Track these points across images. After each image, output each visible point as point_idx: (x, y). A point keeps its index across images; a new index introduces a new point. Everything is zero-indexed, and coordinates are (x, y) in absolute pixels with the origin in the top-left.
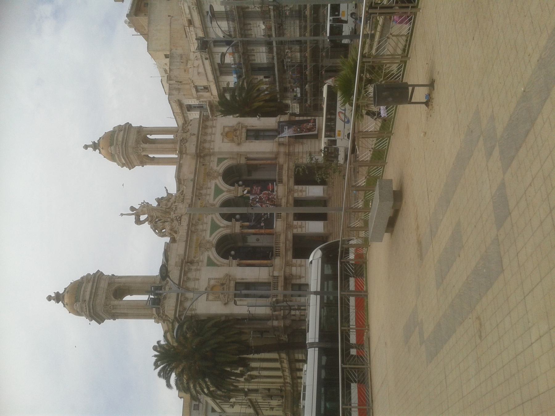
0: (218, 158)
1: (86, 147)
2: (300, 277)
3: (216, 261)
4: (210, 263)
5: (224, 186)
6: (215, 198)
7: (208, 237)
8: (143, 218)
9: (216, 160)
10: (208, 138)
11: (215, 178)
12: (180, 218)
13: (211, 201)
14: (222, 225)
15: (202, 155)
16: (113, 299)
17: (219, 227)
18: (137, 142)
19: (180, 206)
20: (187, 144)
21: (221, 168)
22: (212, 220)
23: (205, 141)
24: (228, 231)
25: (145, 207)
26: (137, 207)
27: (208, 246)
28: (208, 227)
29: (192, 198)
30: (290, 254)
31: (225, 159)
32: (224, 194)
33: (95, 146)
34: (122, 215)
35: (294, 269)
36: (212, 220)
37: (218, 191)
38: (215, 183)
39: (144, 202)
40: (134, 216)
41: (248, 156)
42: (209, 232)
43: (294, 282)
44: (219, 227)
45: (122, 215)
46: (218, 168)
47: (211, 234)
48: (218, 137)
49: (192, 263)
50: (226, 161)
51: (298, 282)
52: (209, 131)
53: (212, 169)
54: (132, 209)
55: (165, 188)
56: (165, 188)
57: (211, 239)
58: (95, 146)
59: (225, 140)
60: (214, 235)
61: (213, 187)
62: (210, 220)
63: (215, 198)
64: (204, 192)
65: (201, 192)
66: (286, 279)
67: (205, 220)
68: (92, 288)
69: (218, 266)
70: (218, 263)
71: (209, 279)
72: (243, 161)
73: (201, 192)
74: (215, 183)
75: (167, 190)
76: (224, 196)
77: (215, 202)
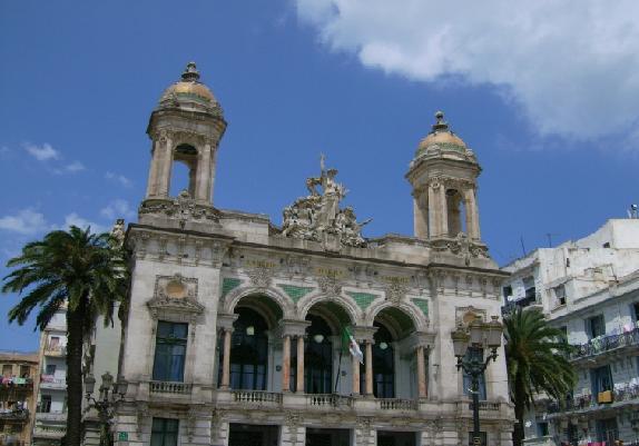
0: (427, 301)
4: (228, 285)
5: (373, 310)
10: (462, 285)
15: (431, 275)
16: (178, 143)
17: (296, 300)
18: (447, 182)
20: (449, 252)
21: (407, 303)
23: (456, 279)
24: (288, 314)
30: (237, 418)
31: (426, 314)
38: (380, 296)
42: (288, 282)
43: (182, 424)
49: (231, 253)
50: (421, 313)
52: (476, 286)
53: (406, 292)
59: (460, 314)
60: (281, 290)
61: (372, 292)
64: (363, 276)
65: (363, 273)
66: (185, 408)
67: (309, 278)
71: (194, 280)
72: (423, 342)
73: (363, 273)
77: (343, 294)
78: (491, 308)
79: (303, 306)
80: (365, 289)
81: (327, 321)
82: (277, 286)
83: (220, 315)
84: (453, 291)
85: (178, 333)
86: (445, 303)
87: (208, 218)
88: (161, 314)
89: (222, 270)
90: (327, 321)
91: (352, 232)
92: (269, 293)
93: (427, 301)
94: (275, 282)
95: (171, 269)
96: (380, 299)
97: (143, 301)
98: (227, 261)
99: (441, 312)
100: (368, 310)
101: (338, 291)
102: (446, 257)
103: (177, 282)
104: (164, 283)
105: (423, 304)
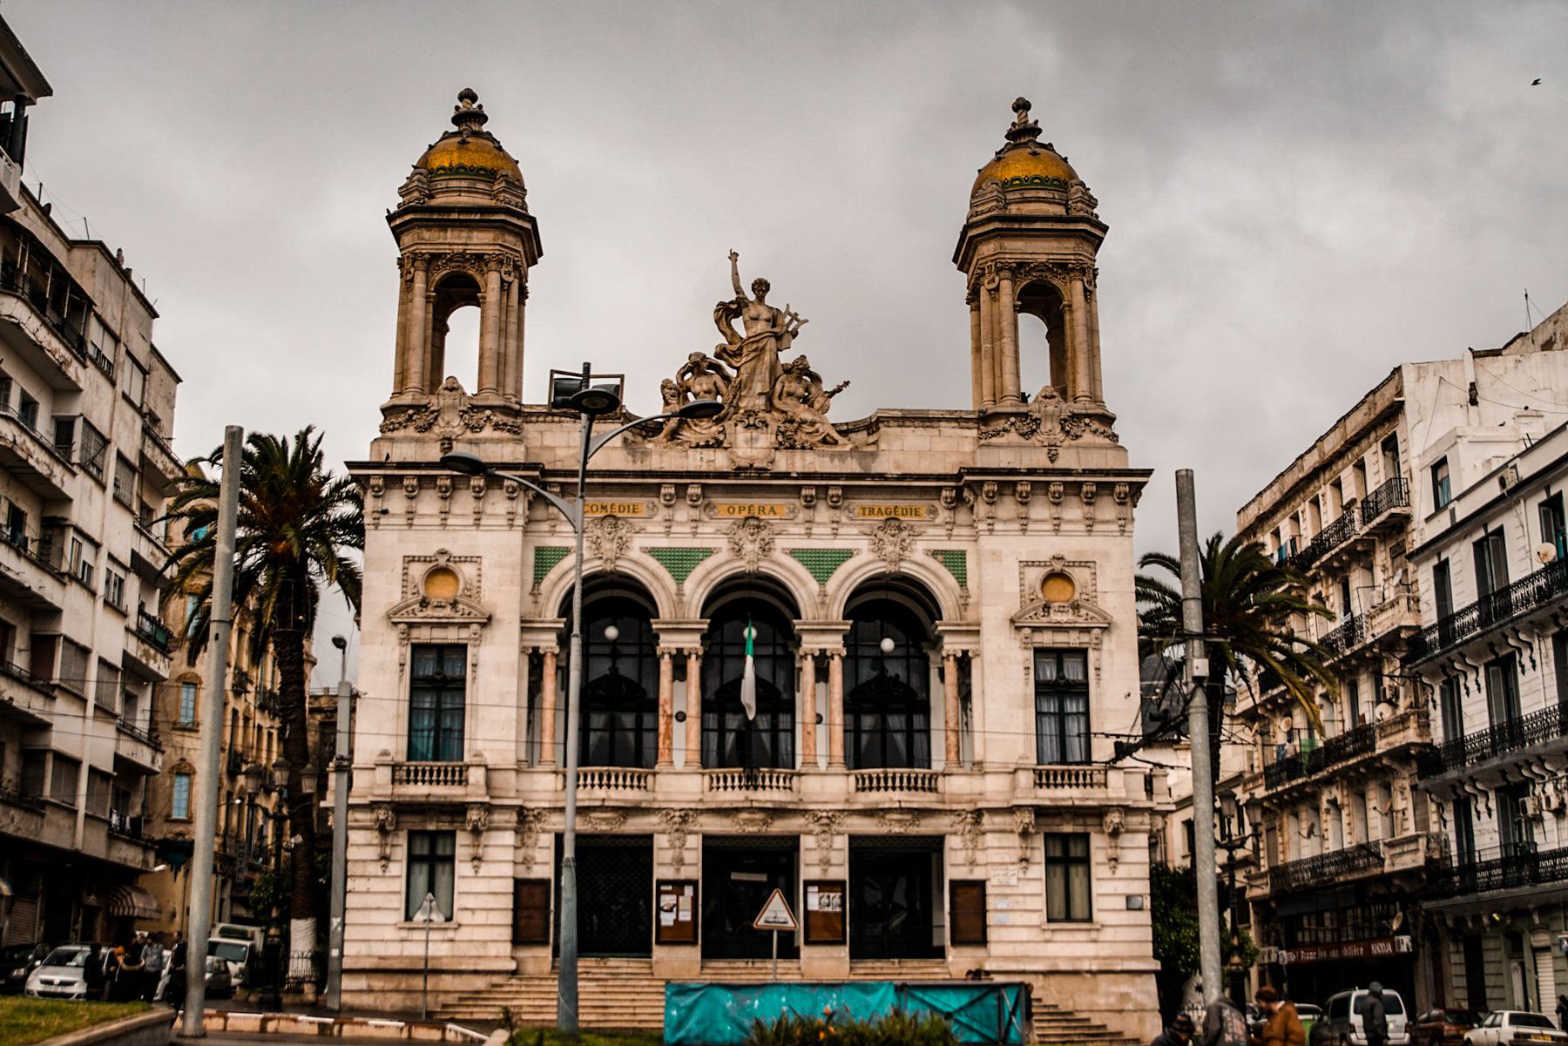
1: (1022, 106)
2: (476, 858)
3: (553, 575)
4: (544, 560)
6: (794, 553)
7: (638, 542)
9: (953, 546)
11: (878, 546)
12: (718, 444)
13: (781, 543)
14: (688, 585)
17: (680, 578)
18: (1018, 269)
19: (765, 439)
20: (1013, 437)
22: (708, 552)
25: (781, 329)
27: (606, 546)
28: (681, 540)
29: (787, 475)
31: (962, 580)
32: (814, 585)
33: (1023, 135)
34: (734, 256)
35: (509, 838)
36: (708, 552)
37: (823, 560)
38: (859, 551)
39: (802, 322)
41: (975, 664)
42: (663, 543)
44: (680, 578)
45: (734, 256)
46: (919, 556)
47: (655, 552)
48: (1044, 546)
49: (538, 501)
50: (951, 580)
51: (462, 852)
54: (761, 287)
55: (847, 383)
56: (847, 383)
57: (635, 554)
58: (1023, 135)
60: (653, 563)
61: (839, 544)
62: (707, 544)
63: (794, 553)
69: (538, 580)
70: (546, 584)
74: (859, 551)
75: (839, 390)
76: (804, 587)
77: (777, 555)
78: (1106, 555)
79: (696, 588)
80: (822, 541)
81: (751, 608)
82: (643, 544)
83: (526, 626)
84: (1016, 526)
85: (451, 671)
86: (996, 555)
87: (497, 427)
88: (415, 633)
89: (525, 532)
90: (751, 608)
91: (808, 416)
92: (625, 566)
93: (962, 554)
94: (638, 542)
95: (428, 542)
96: (864, 558)
97: (382, 610)
98: (540, 512)
99: (992, 574)
100: (832, 585)
101: (766, 549)
102: (1009, 452)
103: (441, 570)
104: (418, 570)
105: (955, 561)
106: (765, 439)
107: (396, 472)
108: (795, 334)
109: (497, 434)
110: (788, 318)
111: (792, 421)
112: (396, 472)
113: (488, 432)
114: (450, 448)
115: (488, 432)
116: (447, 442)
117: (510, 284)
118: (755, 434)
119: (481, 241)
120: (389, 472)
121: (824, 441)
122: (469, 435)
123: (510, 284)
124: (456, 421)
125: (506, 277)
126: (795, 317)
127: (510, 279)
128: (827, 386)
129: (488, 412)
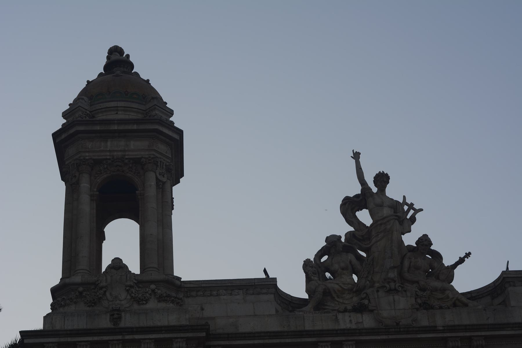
8: (364, 217)
26: (393, 192)
34: (356, 156)
39: (417, 211)
40: (356, 189)
45: (356, 156)
54: (382, 179)
55: (468, 255)
56: (468, 255)
68: (121, 122)
75: (461, 261)
87: (161, 299)
106: (403, 302)
107: (69, 339)
108: (413, 220)
109: (162, 305)
110: (406, 208)
111: (423, 290)
112: (69, 339)
113: (152, 304)
114: (120, 318)
115: (152, 304)
116: (116, 314)
117: (164, 183)
118: (396, 297)
119: (137, 147)
120: (62, 340)
121: (455, 305)
122: (136, 306)
123: (164, 183)
124: (123, 295)
125: (160, 177)
126: (411, 206)
127: (164, 179)
128: (447, 262)
129: (153, 286)
